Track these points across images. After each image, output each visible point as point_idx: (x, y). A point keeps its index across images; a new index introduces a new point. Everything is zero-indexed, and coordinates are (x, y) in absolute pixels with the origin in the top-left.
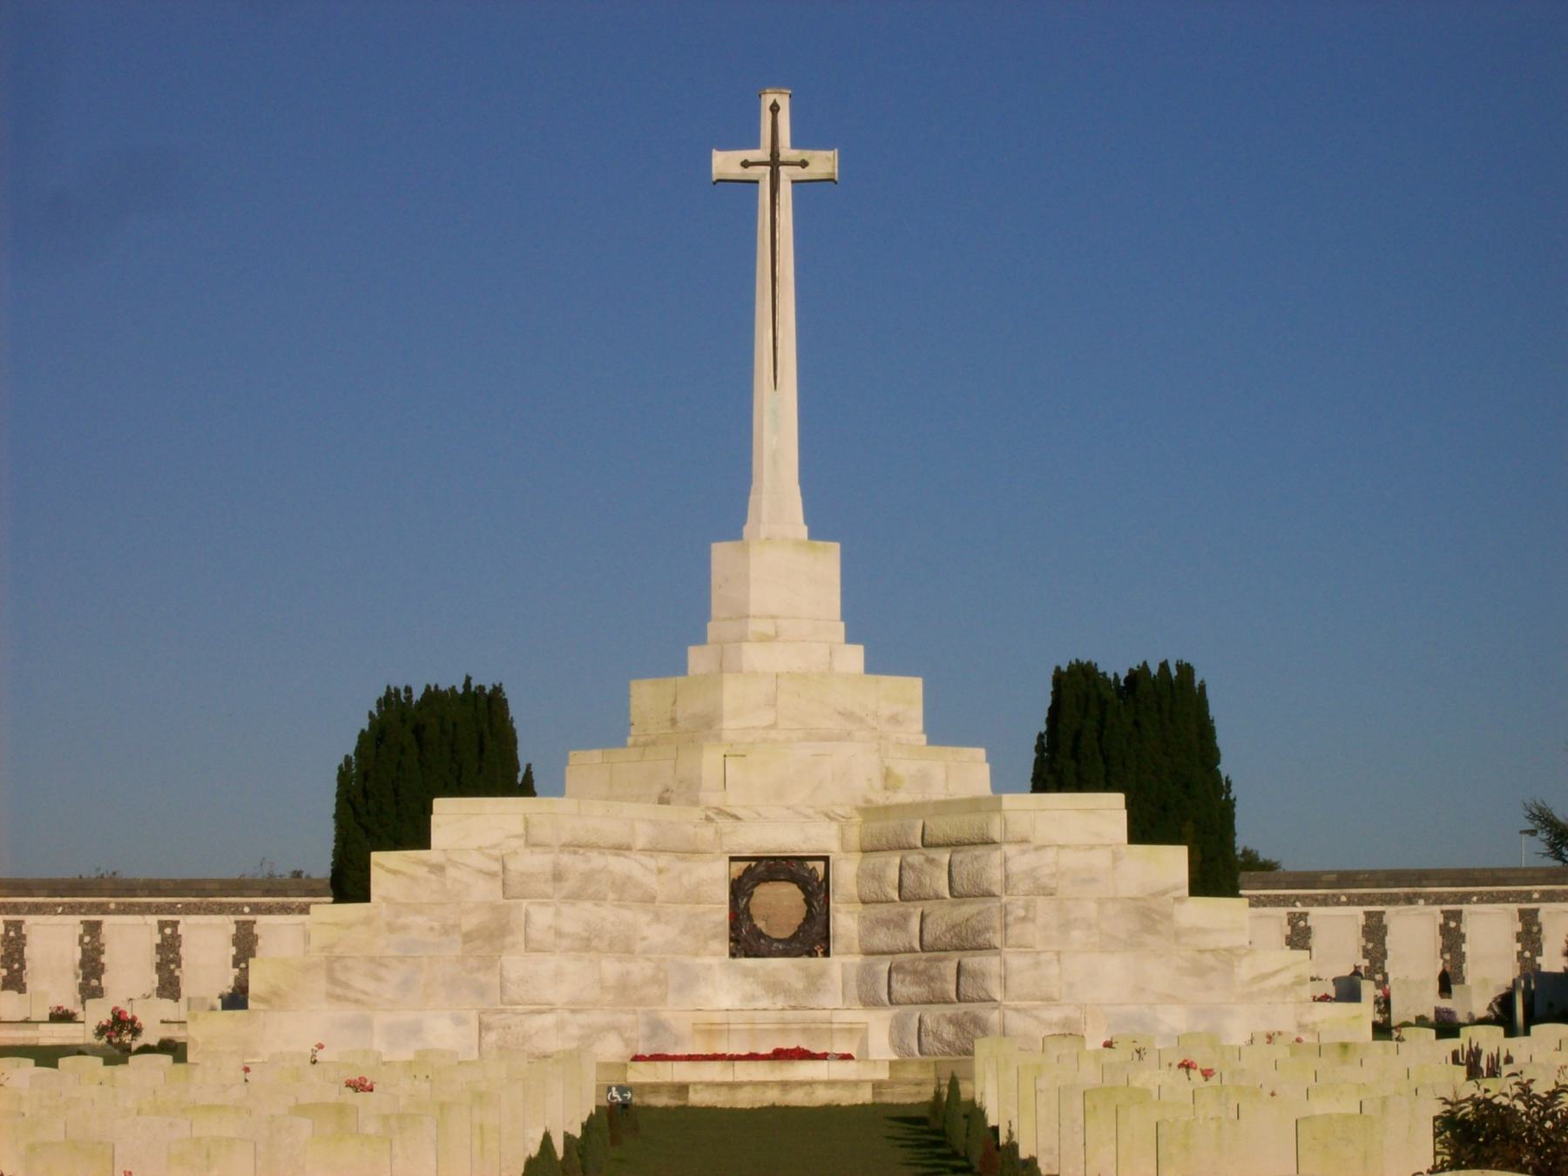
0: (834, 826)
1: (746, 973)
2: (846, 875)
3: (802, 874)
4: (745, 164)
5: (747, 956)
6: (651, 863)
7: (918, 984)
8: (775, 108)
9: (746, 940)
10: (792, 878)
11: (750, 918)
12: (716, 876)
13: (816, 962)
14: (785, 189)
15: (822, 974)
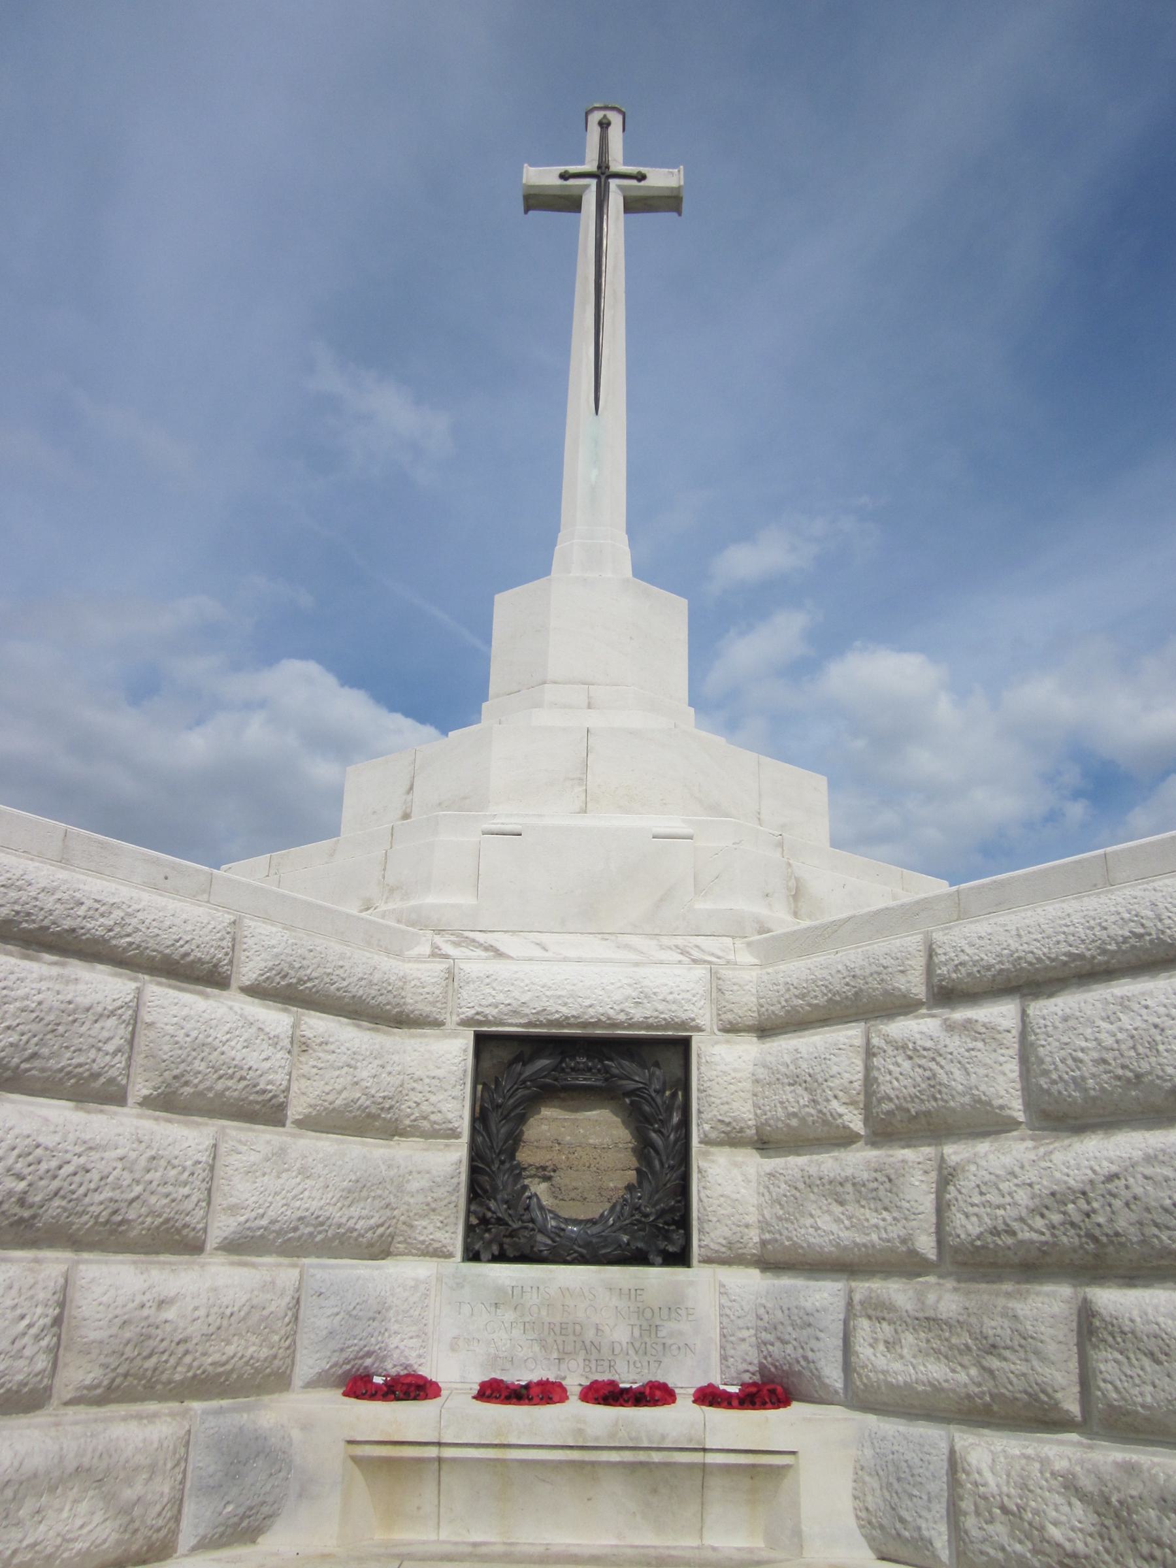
0: (701, 972)
1: (501, 1299)
2: (727, 1074)
3: (630, 1071)
4: (564, 176)
5: (501, 1257)
6: (276, 1019)
7: (950, 1354)
8: (604, 125)
9: (501, 1223)
10: (605, 1092)
11: (518, 1172)
12: (439, 1070)
13: (655, 1277)
14: (615, 201)
15: (674, 1307)
